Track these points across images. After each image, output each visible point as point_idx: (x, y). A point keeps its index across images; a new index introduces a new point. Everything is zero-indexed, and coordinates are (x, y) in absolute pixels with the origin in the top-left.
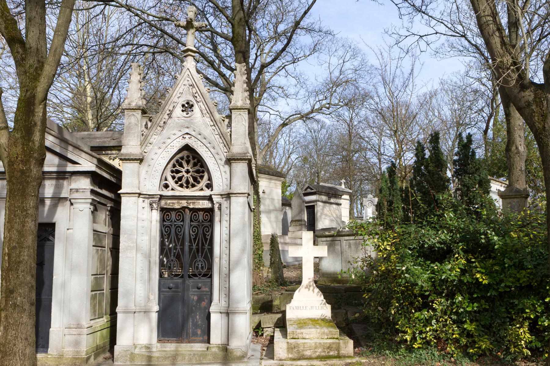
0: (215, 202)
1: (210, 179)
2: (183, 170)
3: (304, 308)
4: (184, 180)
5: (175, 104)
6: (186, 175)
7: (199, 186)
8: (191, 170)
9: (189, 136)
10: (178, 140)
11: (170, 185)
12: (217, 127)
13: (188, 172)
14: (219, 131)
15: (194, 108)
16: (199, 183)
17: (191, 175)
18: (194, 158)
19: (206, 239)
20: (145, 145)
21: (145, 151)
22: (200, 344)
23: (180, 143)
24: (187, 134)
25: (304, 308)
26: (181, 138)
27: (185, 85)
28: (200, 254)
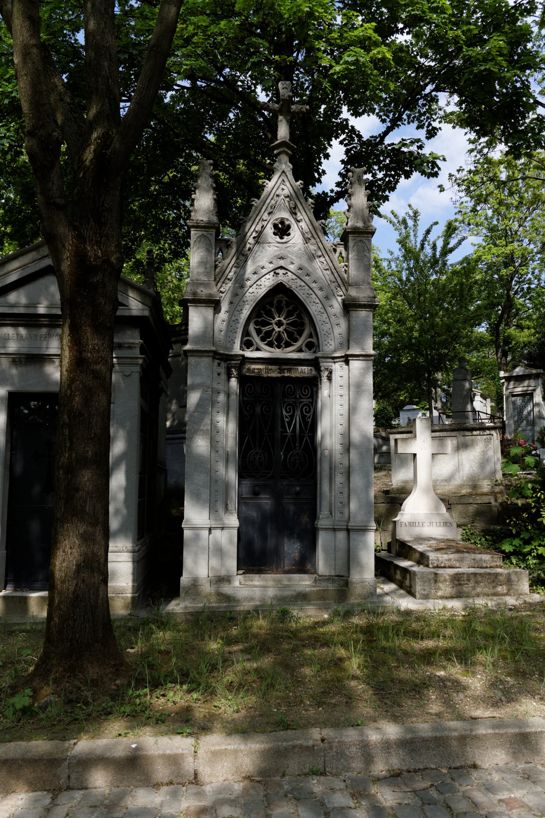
0: (322, 368)
1: (314, 333)
2: (273, 322)
3: (421, 524)
4: (274, 335)
5: (265, 223)
6: (277, 329)
7: (297, 345)
8: (284, 321)
9: (284, 271)
10: (267, 276)
11: (254, 343)
12: (327, 258)
13: (279, 324)
14: (331, 265)
15: (291, 231)
16: (296, 340)
17: (285, 330)
18: (259, 315)
19: (306, 423)
20: (222, 280)
21: (222, 289)
22: (299, 575)
23: (271, 280)
24: (281, 268)
25: (421, 524)
26: (272, 273)
27: (278, 196)
28: (297, 444)
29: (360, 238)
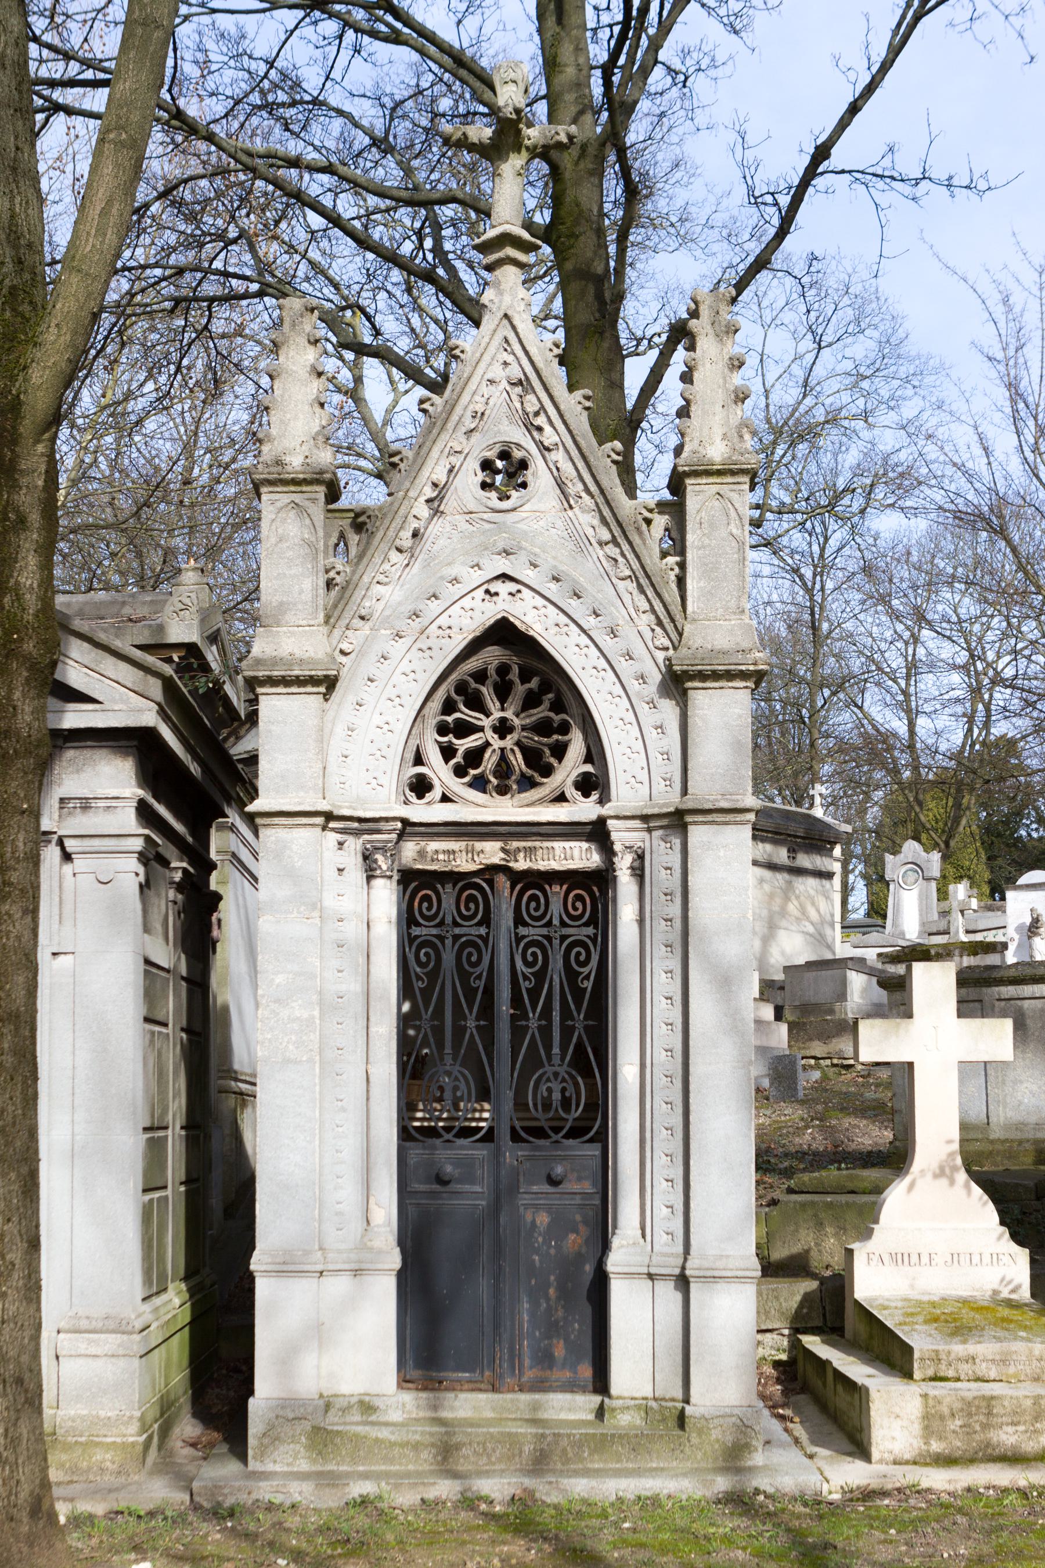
0: (617, 847)
1: (595, 753)
2: (486, 722)
3: (925, 1259)
4: (490, 760)
6: (496, 743)
8: (517, 722)
9: (512, 587)
10: (466, 602)
11: (436, 782)
12: (626, 547)
13: (503, 729)
15: (529, 475)
16: (547, 771)
17: (518, 743)
19: (578, 993)
20: (343, 623)
21: (345, 646)
22: (568, 1396)
24: (504, 577)
25: (925, 1259)
26: (480, 593)
27: (491, 382)
29: (715, 488)
